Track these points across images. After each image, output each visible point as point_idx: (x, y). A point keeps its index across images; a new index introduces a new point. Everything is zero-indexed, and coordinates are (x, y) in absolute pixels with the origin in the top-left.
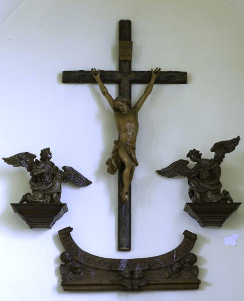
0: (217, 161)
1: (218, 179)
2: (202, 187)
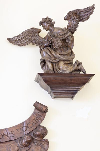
0: (70, 30)
1: (71, 49)
2: (55, 57)
